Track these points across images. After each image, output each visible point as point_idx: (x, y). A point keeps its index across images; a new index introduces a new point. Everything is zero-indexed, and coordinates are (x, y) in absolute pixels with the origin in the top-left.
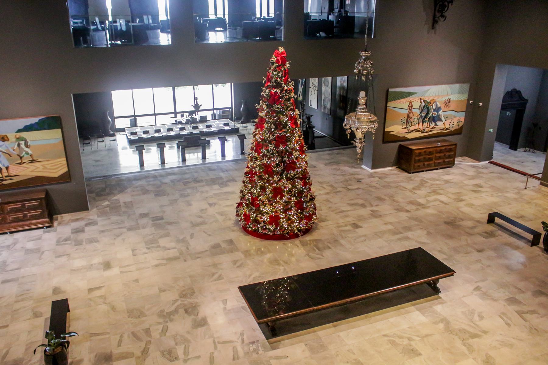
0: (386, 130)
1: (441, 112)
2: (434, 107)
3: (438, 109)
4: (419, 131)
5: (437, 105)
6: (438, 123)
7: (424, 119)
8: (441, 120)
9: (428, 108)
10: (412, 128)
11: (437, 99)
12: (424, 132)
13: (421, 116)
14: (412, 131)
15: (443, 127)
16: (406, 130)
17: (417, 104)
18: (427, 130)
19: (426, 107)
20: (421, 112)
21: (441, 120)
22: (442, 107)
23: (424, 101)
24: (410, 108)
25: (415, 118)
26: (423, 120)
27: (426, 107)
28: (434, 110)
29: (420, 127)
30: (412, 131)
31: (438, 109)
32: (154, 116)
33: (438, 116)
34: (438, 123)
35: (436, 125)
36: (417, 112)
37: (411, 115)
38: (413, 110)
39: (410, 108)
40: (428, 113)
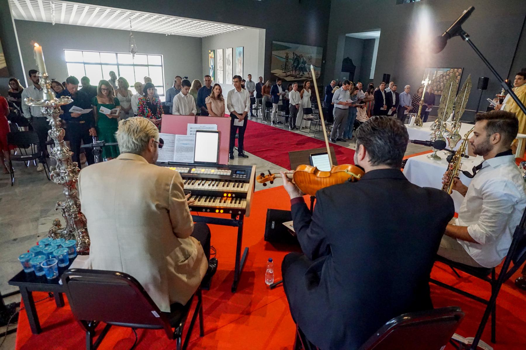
0: (272, 72)
1: (306, 65)
2: (302, 61)
3: (304, 63)
5: (303, 59)
7: (296, 68)
8: (307, 71)
9: (298, 60)
10: (288, 73)
11: (303, 55)
13: (294, 66)
14: (288, 76)
15: (308, 76)
16: (284, 74)
17: (291, 56)
18: (298, 76)
19: (297, 59)
20: (294, 63)
21: (307, 71)
22: (307, 61)
23: (296, 55)
24: (287, 58)
25: (290, 66)
26: (296, 68)
27: (297, 59)
28: (302, 62)
29: (294, 73)
30: (288, 76)
31: (304, 63)
32: (102, 62)
33: (305, 67)
35: (303, 74)
37: (288, 64)
39: (287, 58)
40: (298, 64)
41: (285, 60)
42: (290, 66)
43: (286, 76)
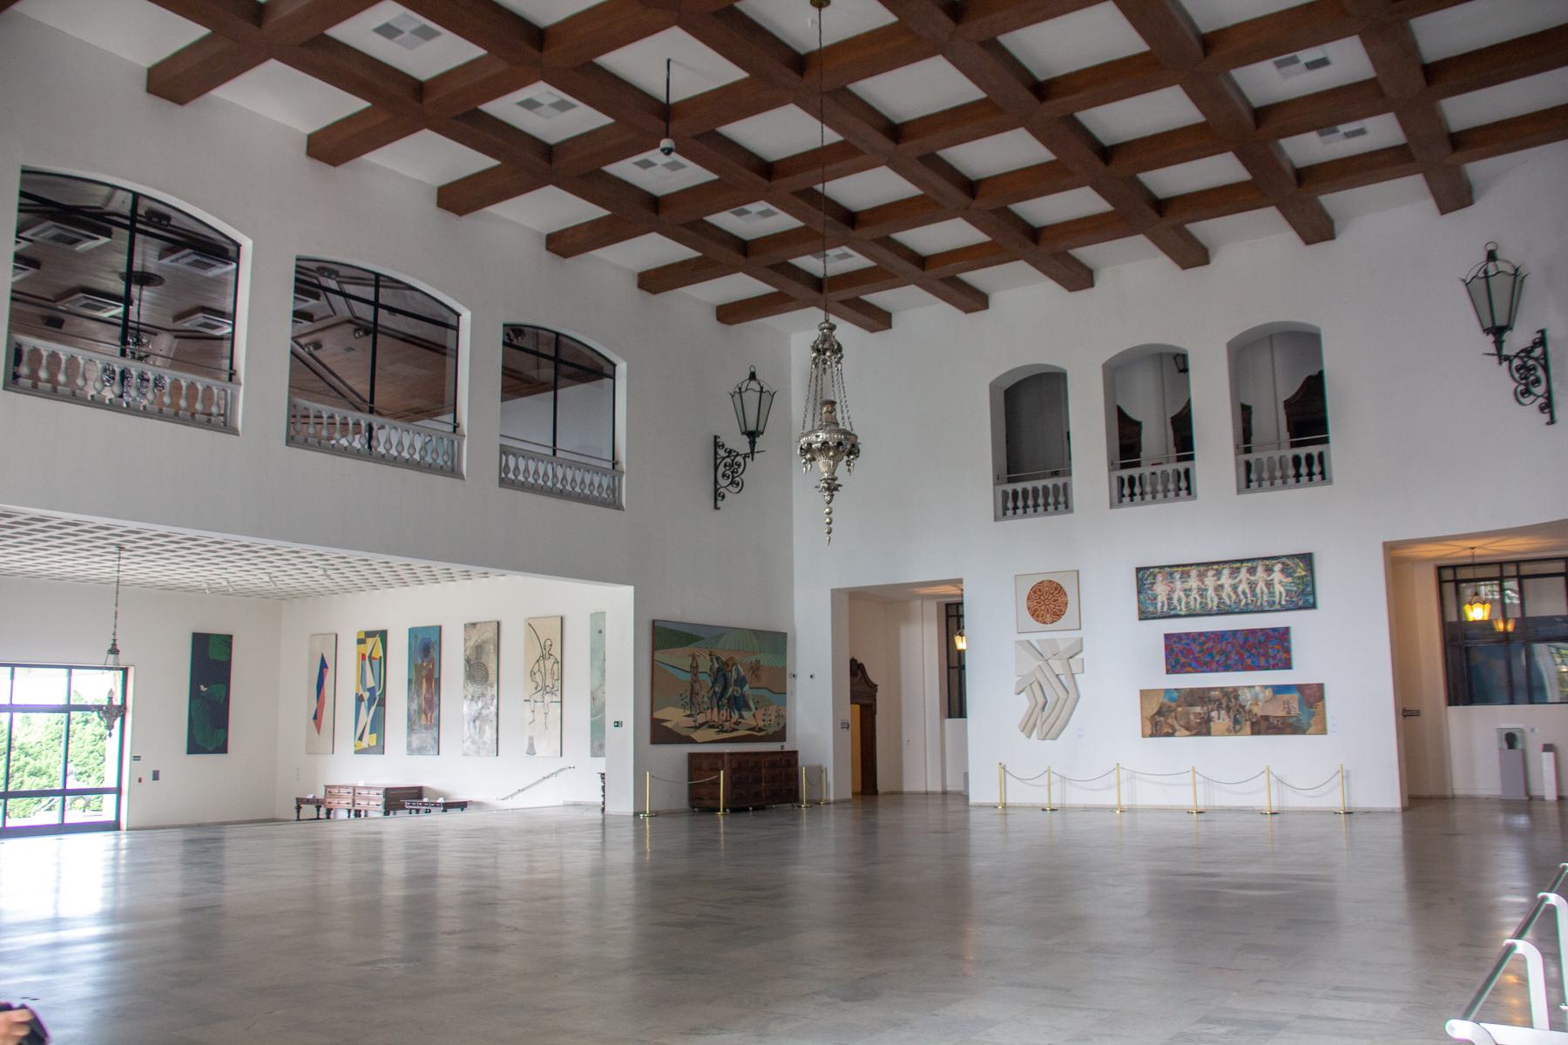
1: (746, 688)
4: (712, 727)
6: (745, 714)
8: (749, 708)
10: (701, 718)
11: (737, 658)
12: (722, 731)
15: (753, 723)
16: (690, 722)
17: (705, 664)
21: (749, 708)
22: (748, 678)
24: (694, 669)
31: (741, 681)
33: (743, 695)
34: (745, 714)
35: (741, 716)
36: (706, 680)
37: (697, 687)
38: (702, 677)
39: (694, 669)
40: (725, 688)
41: (688, 677)
42: (704, 696)
43: (696, 728)
